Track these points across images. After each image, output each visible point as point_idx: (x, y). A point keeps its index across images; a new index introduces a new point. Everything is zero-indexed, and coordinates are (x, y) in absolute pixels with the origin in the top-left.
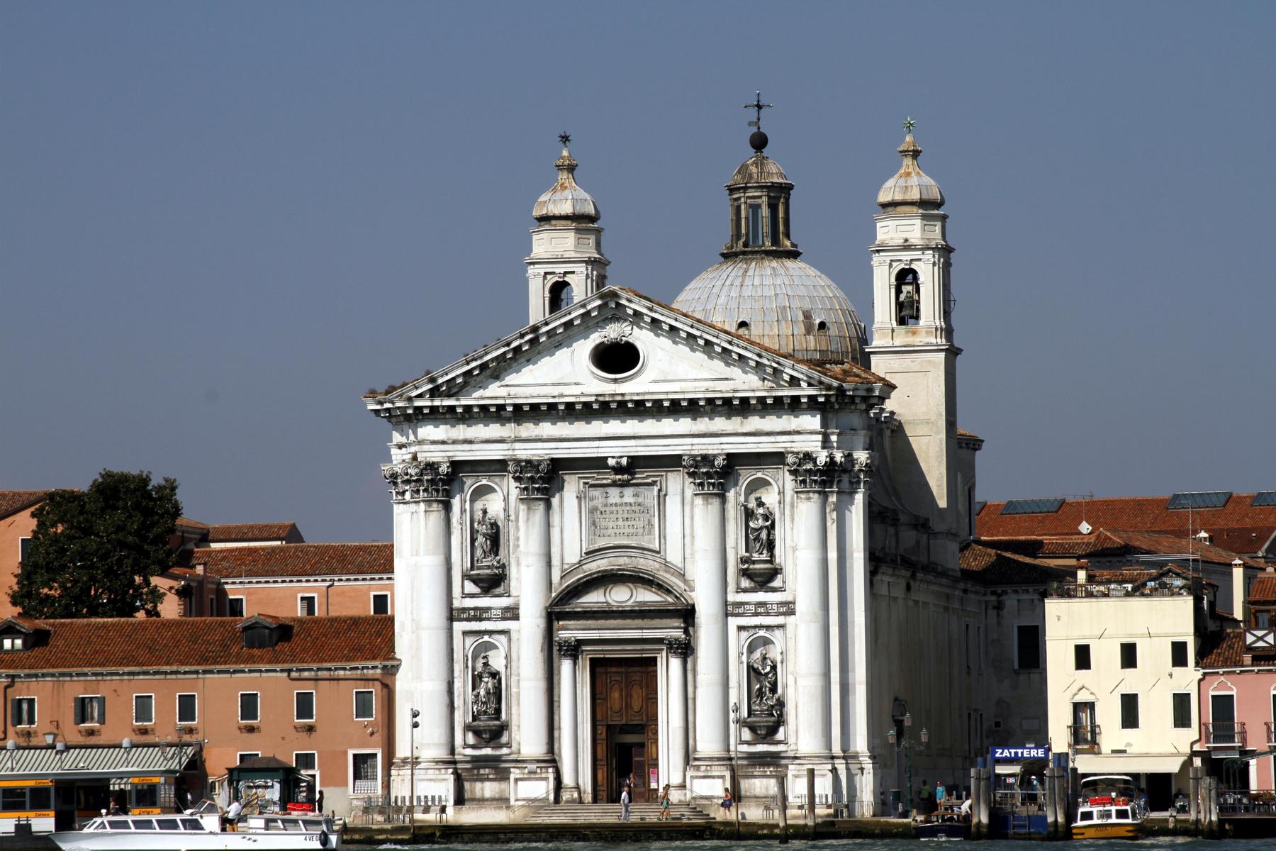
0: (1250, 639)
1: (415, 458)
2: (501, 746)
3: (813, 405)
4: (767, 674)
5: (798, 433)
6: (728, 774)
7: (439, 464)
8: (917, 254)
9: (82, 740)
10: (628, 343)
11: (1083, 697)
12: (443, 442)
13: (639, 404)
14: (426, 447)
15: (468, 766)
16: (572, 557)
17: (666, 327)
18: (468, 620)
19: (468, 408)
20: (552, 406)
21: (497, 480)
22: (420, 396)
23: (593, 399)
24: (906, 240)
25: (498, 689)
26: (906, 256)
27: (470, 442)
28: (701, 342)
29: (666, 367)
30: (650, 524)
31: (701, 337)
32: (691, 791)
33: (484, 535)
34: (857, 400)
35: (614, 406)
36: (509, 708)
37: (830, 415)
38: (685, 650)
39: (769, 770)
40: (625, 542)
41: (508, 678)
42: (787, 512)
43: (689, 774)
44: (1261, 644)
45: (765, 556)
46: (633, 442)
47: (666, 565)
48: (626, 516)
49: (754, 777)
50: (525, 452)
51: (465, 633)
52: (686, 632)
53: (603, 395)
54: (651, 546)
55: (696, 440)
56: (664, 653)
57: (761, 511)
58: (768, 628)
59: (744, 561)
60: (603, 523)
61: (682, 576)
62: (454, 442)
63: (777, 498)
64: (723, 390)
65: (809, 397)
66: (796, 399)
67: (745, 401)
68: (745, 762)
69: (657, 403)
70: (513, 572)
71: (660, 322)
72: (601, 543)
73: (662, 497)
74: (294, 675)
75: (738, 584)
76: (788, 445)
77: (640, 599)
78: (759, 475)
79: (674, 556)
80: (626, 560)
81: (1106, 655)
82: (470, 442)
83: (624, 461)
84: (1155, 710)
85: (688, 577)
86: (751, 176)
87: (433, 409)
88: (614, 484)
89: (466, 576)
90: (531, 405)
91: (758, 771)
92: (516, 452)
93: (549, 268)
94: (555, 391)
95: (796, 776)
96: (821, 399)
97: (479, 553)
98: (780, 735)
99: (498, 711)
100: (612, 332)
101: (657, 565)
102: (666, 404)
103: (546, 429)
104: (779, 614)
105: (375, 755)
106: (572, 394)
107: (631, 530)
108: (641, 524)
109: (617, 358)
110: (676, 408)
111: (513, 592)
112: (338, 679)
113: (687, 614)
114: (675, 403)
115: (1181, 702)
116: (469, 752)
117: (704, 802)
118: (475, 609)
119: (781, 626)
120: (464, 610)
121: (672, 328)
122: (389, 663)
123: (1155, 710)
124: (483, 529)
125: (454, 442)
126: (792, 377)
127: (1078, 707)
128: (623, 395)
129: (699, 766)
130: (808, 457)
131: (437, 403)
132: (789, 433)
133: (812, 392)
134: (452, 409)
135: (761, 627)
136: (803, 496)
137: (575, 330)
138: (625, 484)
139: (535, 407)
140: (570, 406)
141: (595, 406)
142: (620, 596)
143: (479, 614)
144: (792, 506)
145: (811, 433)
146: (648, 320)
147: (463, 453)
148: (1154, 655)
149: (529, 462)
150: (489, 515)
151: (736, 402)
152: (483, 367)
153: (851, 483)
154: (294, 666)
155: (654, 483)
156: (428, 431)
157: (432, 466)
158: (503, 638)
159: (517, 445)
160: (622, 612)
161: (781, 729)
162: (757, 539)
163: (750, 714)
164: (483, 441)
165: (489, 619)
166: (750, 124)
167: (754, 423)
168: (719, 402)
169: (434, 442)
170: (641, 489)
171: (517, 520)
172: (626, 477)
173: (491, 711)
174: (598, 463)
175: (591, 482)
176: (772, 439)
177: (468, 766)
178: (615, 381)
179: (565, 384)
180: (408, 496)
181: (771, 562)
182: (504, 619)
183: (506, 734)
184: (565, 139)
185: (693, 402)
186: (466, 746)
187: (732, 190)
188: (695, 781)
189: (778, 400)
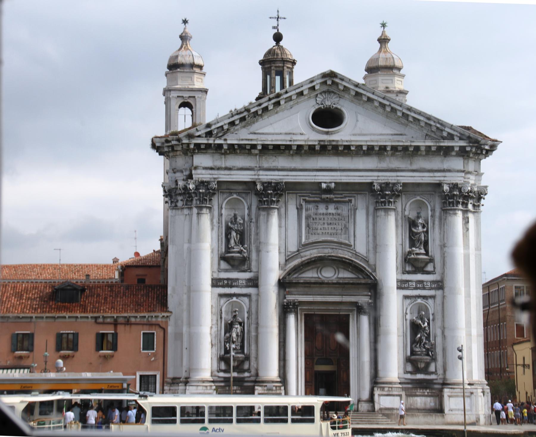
2: (244, 371)
3: (463, 153)
4: (425, 327)
6: (403, 394)
7: (208, 183)
10: (336, 108)
12: (212, 169)
13: (347, 147)
14: (199, 171)
15: (222, 384)
16: (293, 247)
17: (365, 99)
18: (223, 286)
19: (231, 147)
20: (288, 147)
21: (244, 195)
22: (199, 136)
23: (317, 143)
24: (387, 88)
25: (243, 332)
27: (230, 169)
28: (388, 109)
30: (346, 228)
31: (390, 105)
32: (380, 404)
33: (236, 231)
34: (484, 152)
35: (330, 148)
36: (249, 345)
37: (466, 161)
39: (427, 392)
40: (329, 238)
41: (249, 326)
42: (437, 222)
43: (377, 392)
46: (338, 173)
47: (356, 255)
48: (329, 222)
49: (417, 396)
51: (221, 296)
53: (324, 141)
54: (347, 242)
55: (380, 174)
57: (420, 221)
58: (425, 297)
59: (410, 253)
60: (314, 226)
61: (367, 262)
63: (430, 213)
64: (404, 141)
65: (460, 147)
67: (417, 148)
68: (410, 386)
70: (254, 256)
71: (361, 94)
72: (313, 239)
74: (101, 320)
76: (442, 179)
77: (341, 275)
78: (418, 198)
79: (361, 247)
80: (330, 251)
83: (333, 185)
85: (371, 262)
86: (277, 55)
87: (208, 146)
88: (324, 201)
89: (222, 258)
90: (274, 145)
91: (419, 392)
92: (260, 177)
93: (180, 94)
94: (288, 138)
95: (450, 396)
96: (468, 149)
97: (232, 242)
98: (432, 368)
99: (242, 347)
101: (350, 254)
102: (365, 148)
103: (282, 162)
104: (431, 289)
105: (155, 376)
106: (300, 140)
107: (335, 231)
108: (340, 227)
109: (327, 118)
110: (370, 151)
111: (254, 268)
114: (371, 148)
116: (222, 374)
117: (387, 412)
118: (228, 279)
119: (433, 297)
120: (220, 280)
121: (369, 100)
122: (166, 314)
124: (236, 227)
125: (219, 169)
126: (449, 134)
128: (337, 141)
129: (384, 388)
130: (455, 186)
131: (211, 141)
132: (444, 171)
133: (463, 143)
134: (220, 146)
135: (419, 297)
136: (451, 212)
137: (302, 98)
138: (331, 201)
140: (299, 147)
141: (317, 148)
142: (328, 274)
143: (230, 282)
144: (440, 219)
145: (458, 171)
146: (353, 93)
147: (224, 176)
149: (270, 183)
150: (239, 218)
151: (411, 149)
152: (243, 119)
153: (474, 206)
155: (350, 201)
157: (202, 183)
158: (246, 300)
159: (261, 172)
160: (328, 284)
162: (419, 240)
165: (237, 286)
166: (274, 28)
167: (421, 163)
168: (400, 148)
170: (339, 205)
171: (257, 221)
172: (332, 196)
173: (238, 348)
175: (307, 198)
176: (431, 174)
177: (222, 384)
178: (327, 133)
179: (294, 134)
180: (180, 204)
181: (427, 254)
182: (247, 286)
184: (185, 22)
185: (383, 148)
186: (220, 370)
187: (262, 63)
188: (382, 398)
189: (440, 148)
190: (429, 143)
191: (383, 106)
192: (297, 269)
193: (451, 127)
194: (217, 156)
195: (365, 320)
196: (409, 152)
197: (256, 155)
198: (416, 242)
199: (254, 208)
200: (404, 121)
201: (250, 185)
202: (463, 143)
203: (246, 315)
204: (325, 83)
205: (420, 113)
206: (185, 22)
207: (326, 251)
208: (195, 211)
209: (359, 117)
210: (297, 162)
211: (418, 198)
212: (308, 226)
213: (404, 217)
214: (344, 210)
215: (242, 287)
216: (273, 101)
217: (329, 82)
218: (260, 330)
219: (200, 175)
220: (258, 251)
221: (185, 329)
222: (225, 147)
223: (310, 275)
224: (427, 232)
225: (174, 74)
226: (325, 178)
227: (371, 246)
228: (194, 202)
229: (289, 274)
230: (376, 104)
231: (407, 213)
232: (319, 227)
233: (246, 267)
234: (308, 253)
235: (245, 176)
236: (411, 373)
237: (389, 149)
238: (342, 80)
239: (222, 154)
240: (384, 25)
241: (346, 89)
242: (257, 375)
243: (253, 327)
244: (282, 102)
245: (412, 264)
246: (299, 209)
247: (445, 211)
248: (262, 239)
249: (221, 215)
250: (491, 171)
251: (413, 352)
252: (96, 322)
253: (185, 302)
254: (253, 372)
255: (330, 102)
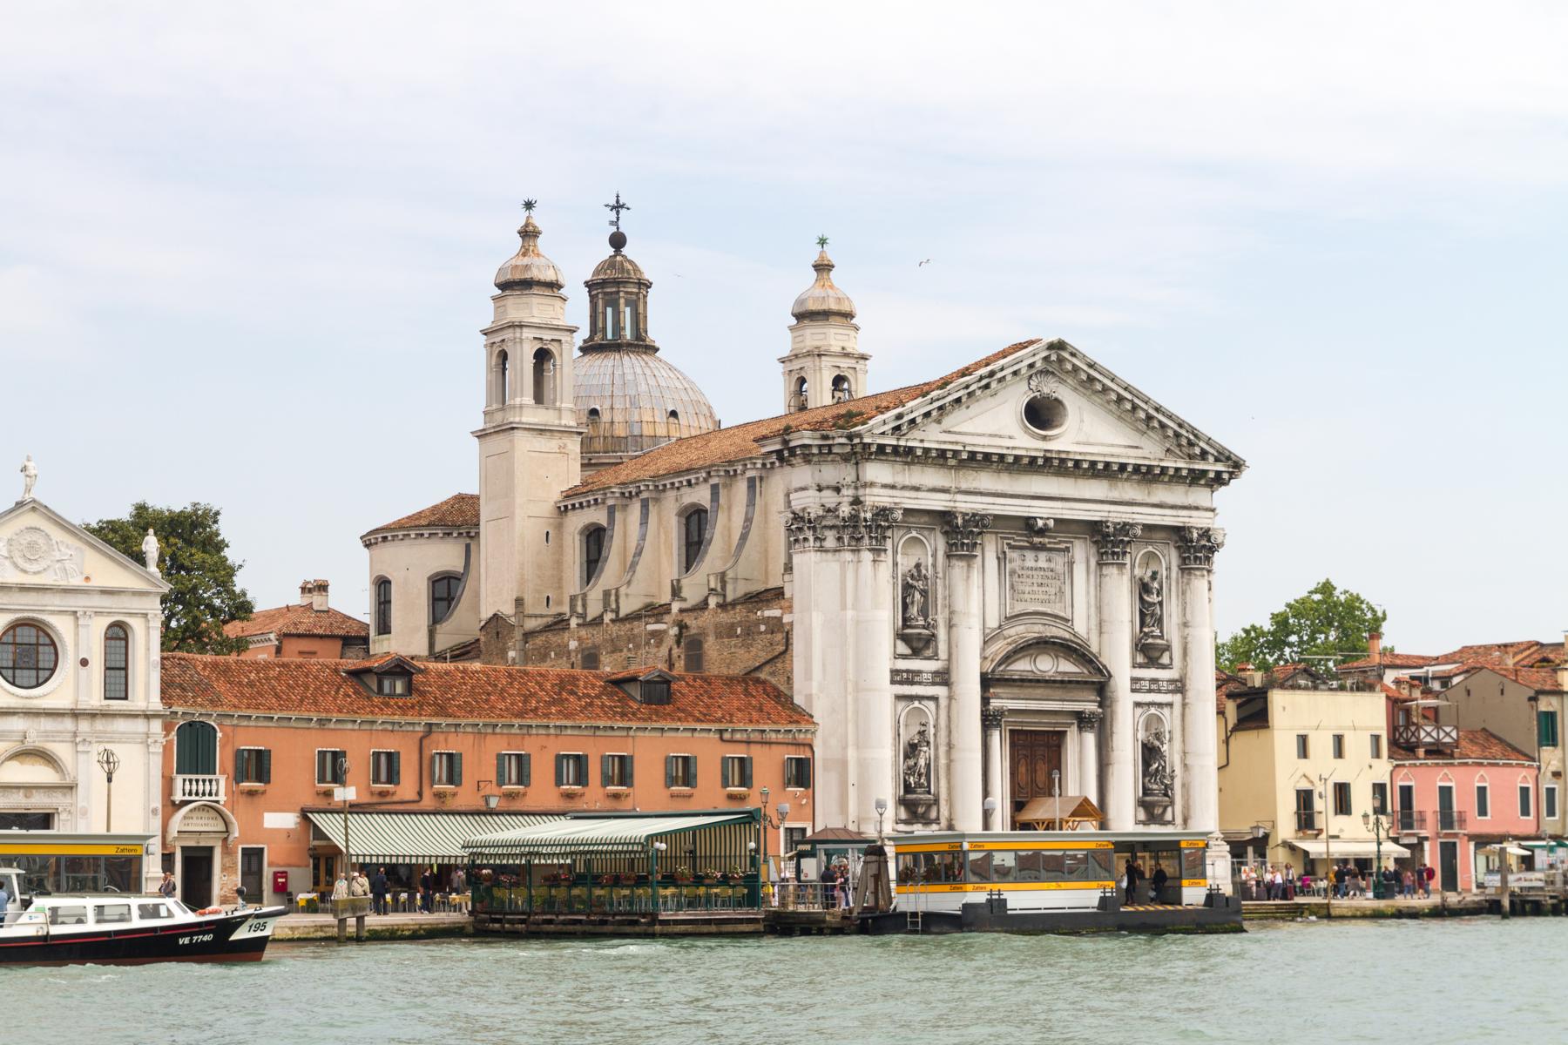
0: (1423, 734)
1: (857, 501)
5: (1197, 508)
7: (891, 510)
8: (851, 362)
9: (505, 805)
11: (1305, 785)
12: (893, 487)
14: (876, 491)
16: (993, 622)
17: (1099, 387)
18: (901, 683)
19: (927, 451)
26: (845, 363)
27: (917, 489)
28: (1128, 406)
29: (1086, 431)
30: (1061, 592)
38: (1100, 724)
41: (936, 749)
44: (1428, 739)
45: (1157, 632)
50: (966, 505)
51: (899, 698)
52: (1101, 705)
55: (1113, 508)
56: (1075, 728)
57: (1156, 585)
58: (1160, 705)
60: (1021, 588)
62: (904, 488)
66: (1204, 472)
67: (1164, 470)
69: (1093, 464)
70: (942, 633)
72: (1020, 608)
73: (1071, 564)
74: (727, 736)
75: (1134, 658)
78: (1150, 548)
79: (1081, 627)
81: (1321, 745)
82: (917, 489)
83: (1051, 523)
84: (1362, 800)
85: (1094, 649)
87: (895, 448)
97: (914, 611)
98: (1168, 816)
100: (1050, 387)
103: (985, 480)
108: (1052, 591)
109: (1041, 414)
111: (943, 654)
112: (771, 743)
113: (1101, 687)
115: (1379, 789)
116: (902, 827)
118: (908, 671)
119: (1170, 705)
121: (1105, 390)
123: (1362, 800)
125: (904, 488)
127: (1298, 792)
131: (902, 443)
133: (1220, 467)
139: (987, 456)
140: (1017, 458)
142: (1046, 665)
143: (910, 678)
148: (1358, 746)
154: (730, 727)
155: (1067, 549)
156: (876, 472)
158: (931, 705)
159: (959, 497)
161: (1169, 810)
163: (1145, 794)
164: (929, 490)
165: (920, 683)
166: (612, 223)
167: (1161, 494)
169: (885, 486)
170: (1053, 555)
174: (1028, 524)
176: (1173, 512)
178: (1045, 438)
180: (830, 542)
181: (1161, 637)
182: (934, 684)
183: (934, 809)
184: (529, 205)
185: (1123, 467)
189: (1191, 471)
190: (1180, 464)
191: (1120, 399)
192: (1008, 658)
193: (1209, 441)
194: (899, 467)
195: (1090, 739)
196: (1147, 475)
197: (952, 467)
198: (1148, 620)
199: (940, 554)
200: (1143, 427)
201: (944, 519)
202: (1220, 467)
203: (932, 731)
204: (1046, 359)
205: (1170, 417)
206: (529, 205)
207: (1038, 628)
208: (867, 556)
209: (1086, 417)
210: (1004, 483)
211: (1150, 548)
212: (1012, 587)
213: (1133, 576)
214: (1059, 562)
215: (927, 684)
216: (984, 382)
217: (1054, 358)
218: (955, 755)
219: (876, 498)
220: (950, 626)
221: (851, 753)
222: (919, 452)
223: (1022, 666)
224: (1161, 603)
225: (525, 299)
226: (1042, 511)
227: (1094, 622)
228: (866, 540)
229: (999, 664)
230: (1114, 397)
231: (1138, 572)
232: (1027, 589)
233: (929, 652)
234: (1012, 631)
235: (938, 503)
236: (1144, 823)
237: (1130, 469)
238: (1073, 355)
239: (906, 463)
240: (823, 242)
241: (1076, 369)
242: (950, 827)
243: (942, 749)
244: (994, 385)
245: (1149, 652)
246: (1002, 559)
247: (1185, 570)
248: (959, 605)
249: (895, 564)
250: (1225, 512)
251: (1146, 792)
252: (721, 738)
253: (850, 708)
254: (944, 822)
255: (1050, 387)
